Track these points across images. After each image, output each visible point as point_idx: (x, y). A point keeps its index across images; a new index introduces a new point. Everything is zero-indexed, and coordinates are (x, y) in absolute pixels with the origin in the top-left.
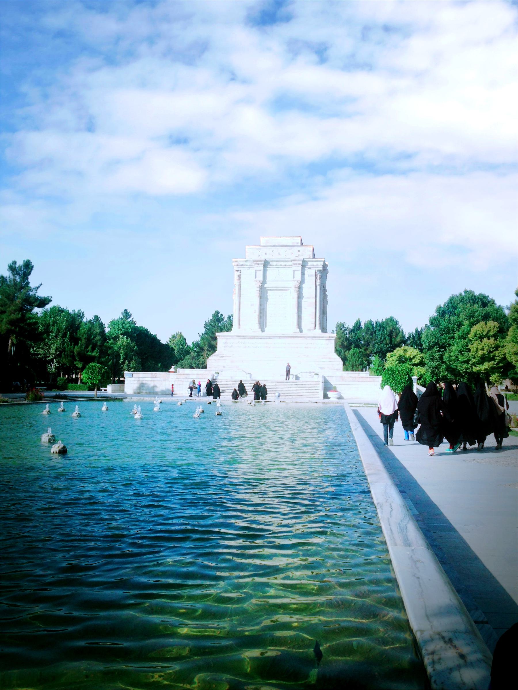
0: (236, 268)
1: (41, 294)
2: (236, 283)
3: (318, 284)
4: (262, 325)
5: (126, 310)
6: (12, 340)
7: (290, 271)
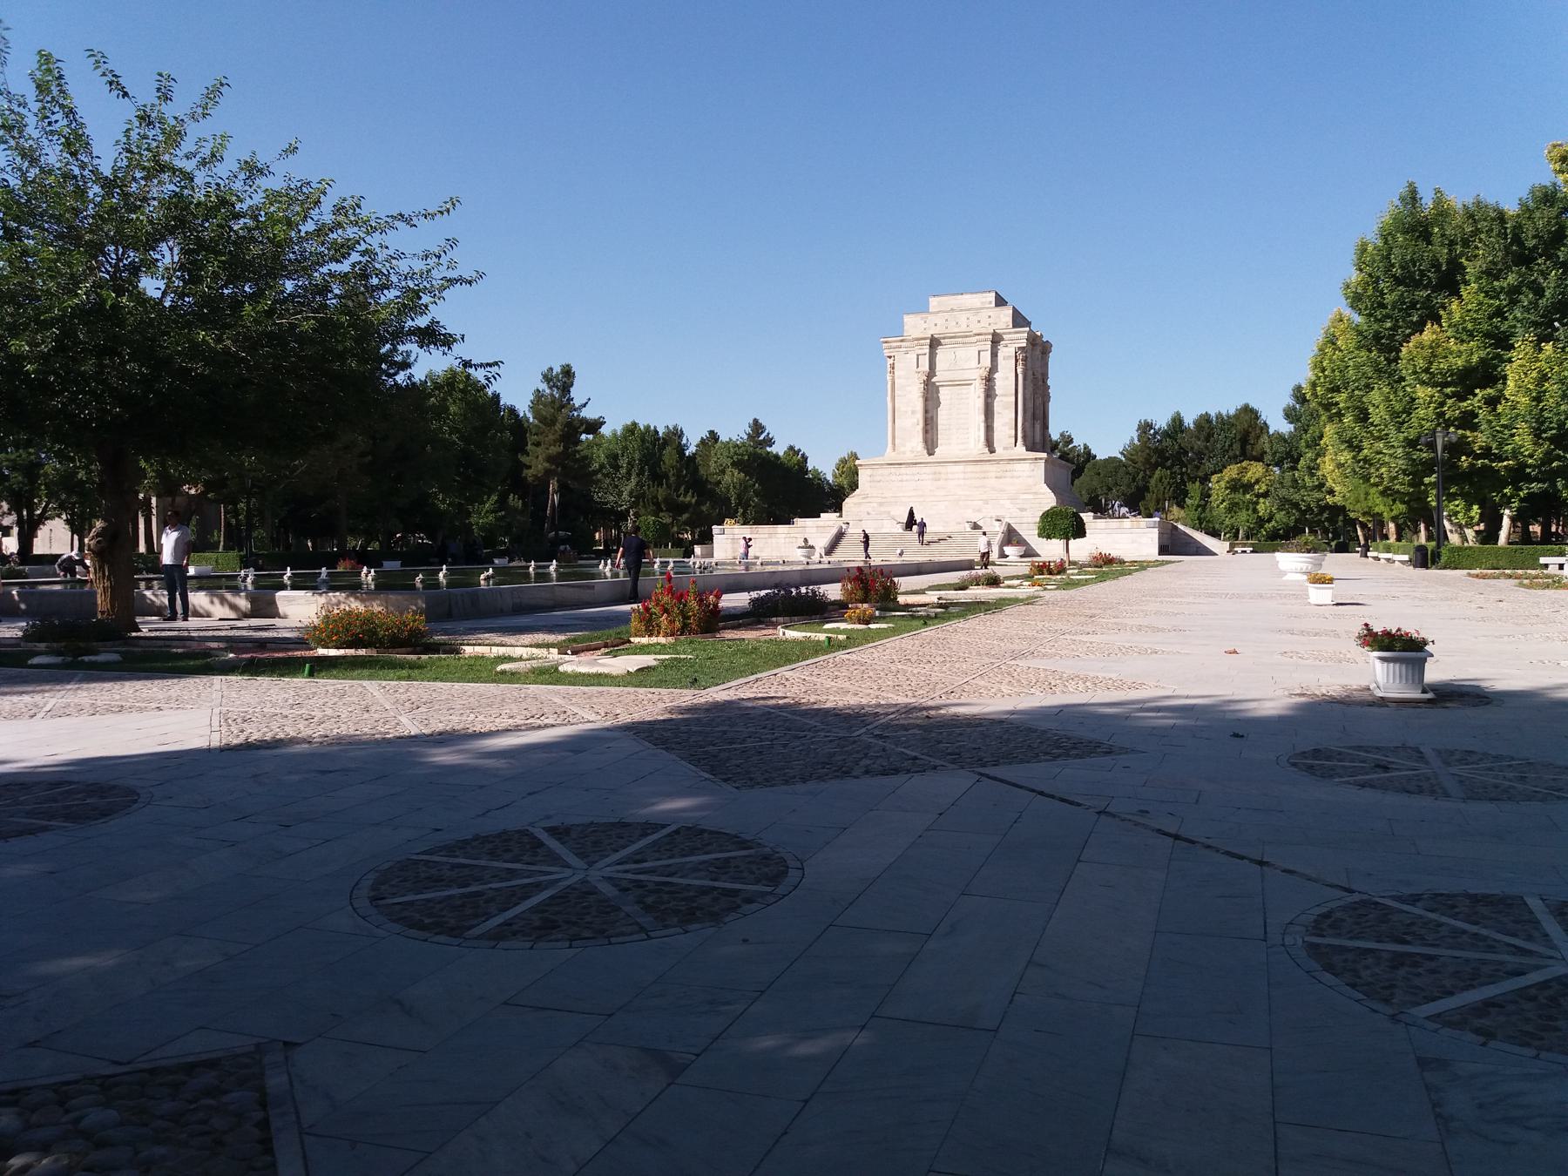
0: (887, 353)
1: (589, 413)
2: (889, 378)
3: (1019, 370)
4: (930, 444)
5: (756, 421)
6: (553, 486)
7: (973, 351)
